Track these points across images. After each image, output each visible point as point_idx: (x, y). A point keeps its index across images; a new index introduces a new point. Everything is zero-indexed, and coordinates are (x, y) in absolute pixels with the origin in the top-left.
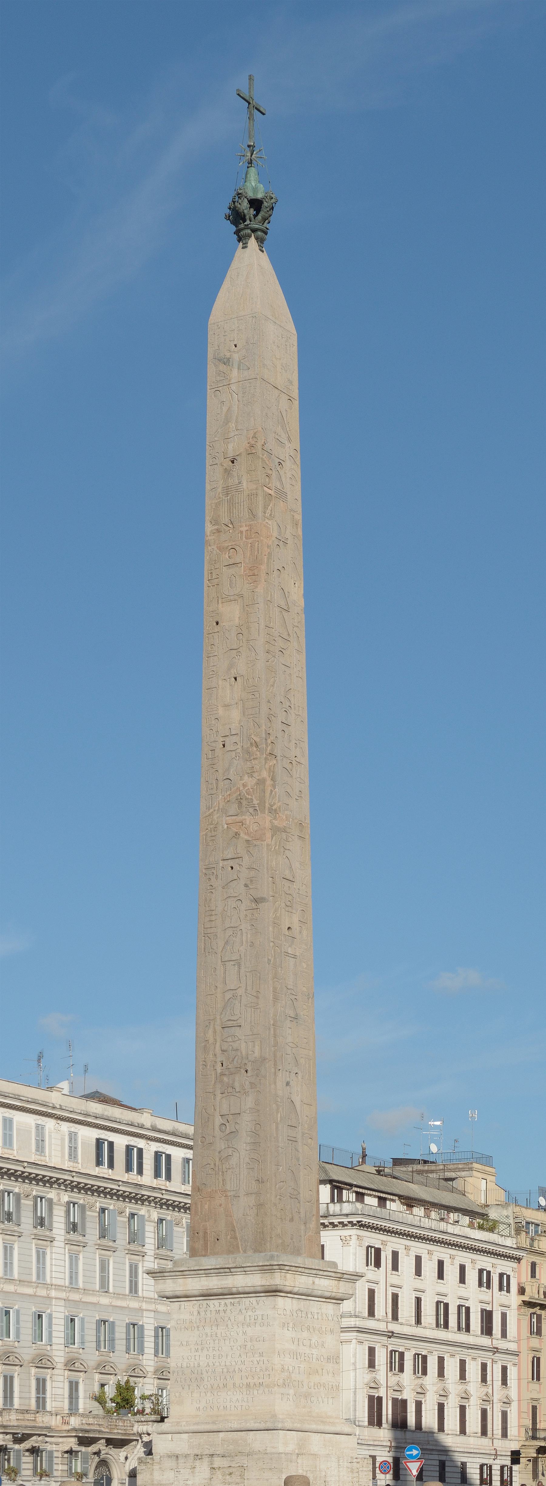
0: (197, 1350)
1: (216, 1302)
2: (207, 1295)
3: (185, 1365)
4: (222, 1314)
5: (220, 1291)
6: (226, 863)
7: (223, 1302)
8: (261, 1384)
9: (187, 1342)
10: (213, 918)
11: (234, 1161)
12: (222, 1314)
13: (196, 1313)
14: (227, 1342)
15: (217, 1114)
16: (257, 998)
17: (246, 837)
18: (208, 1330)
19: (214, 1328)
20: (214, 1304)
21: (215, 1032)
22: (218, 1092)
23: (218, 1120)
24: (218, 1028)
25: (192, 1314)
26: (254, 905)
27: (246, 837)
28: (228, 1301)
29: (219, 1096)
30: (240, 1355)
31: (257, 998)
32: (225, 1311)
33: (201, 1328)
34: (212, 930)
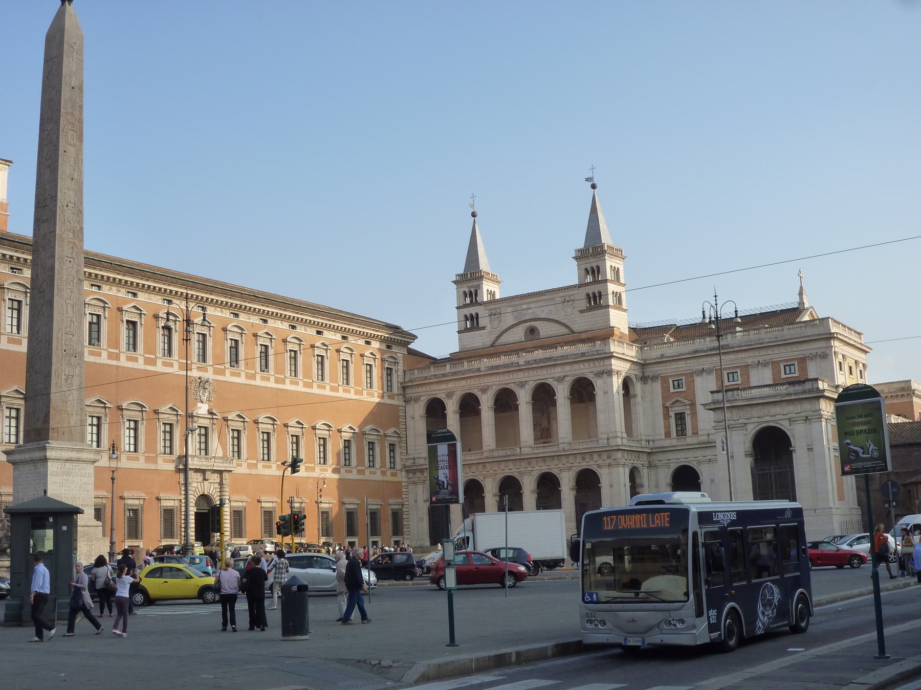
0: (60, 486)
1: (68, 464)
2: (67, 460)
3: (54, 493)
4: (71, 470)
5: (75, 459)
6: (67, 258)
7: (72, 464)
8: (88, 505)
9: (56, 482)
10: (62, 282)
11: (71, 398)
12: (71, 470)
13: (59, 468)
14: (73, 483)
15: (63, 374)
16: (80, 324)
17: (76, 250)
18: (65, 477)
19: (68, 476)
20: (68, 465)
21: (62, 334)
22: (63, 364)
23: (63, 377)
24: (64, 333)
25: (58, 468)
26: (79, 282)
27: (76, 250)
28: (74, 464)
29: (64, 366)
30: (79, 491)
31: (80, 324)
32: (72, 469)
33: (62, 476)
34: (61, 287)
